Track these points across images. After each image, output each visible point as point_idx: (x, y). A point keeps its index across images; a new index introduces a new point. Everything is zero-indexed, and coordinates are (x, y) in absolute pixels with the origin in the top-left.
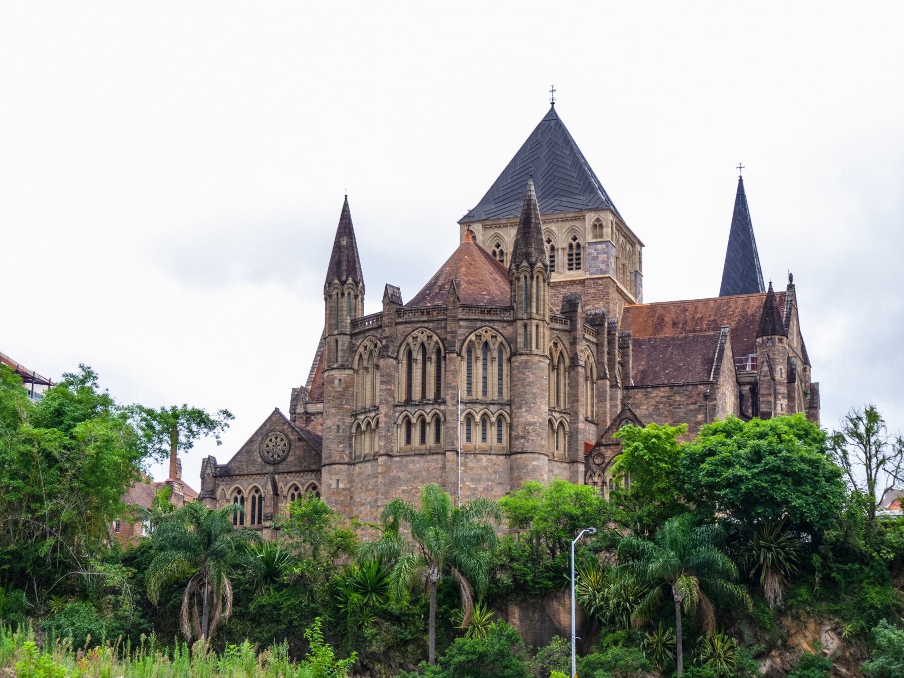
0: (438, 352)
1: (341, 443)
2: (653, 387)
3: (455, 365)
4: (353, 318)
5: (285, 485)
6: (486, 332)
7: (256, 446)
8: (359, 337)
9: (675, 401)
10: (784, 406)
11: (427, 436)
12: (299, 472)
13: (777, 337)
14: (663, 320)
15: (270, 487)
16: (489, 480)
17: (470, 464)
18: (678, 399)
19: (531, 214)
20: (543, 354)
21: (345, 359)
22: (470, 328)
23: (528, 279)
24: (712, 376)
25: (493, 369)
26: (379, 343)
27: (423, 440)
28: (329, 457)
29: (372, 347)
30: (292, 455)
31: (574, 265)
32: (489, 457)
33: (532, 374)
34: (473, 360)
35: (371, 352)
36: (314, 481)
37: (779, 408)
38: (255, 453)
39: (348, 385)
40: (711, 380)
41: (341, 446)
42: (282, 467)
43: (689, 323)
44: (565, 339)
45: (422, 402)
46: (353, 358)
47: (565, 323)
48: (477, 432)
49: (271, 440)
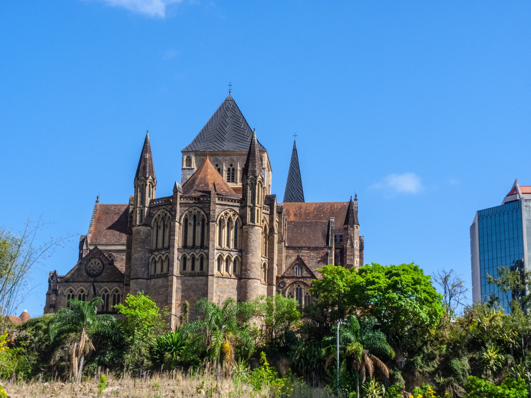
0: (203, 220)
1: (143, 267)
2: (309, 248)
3: (214, 229)
4: (151, 199)
5: (100, 289)
6: (230, 211)
7: (83, 267)
8: (155, 209)
9: (311, 256)
10: (358, 262)
11: (195, 267)
12: (109, 282)
13: (355, 225)
14: (288, 212)
15: (92, 290)
16: (229, 292)
17: (220, 283)
18: (312, 254)
19: (255, 149)
20: (260, 225)
21: (147, 221)
22: (221, 209)
23: (254, 184)
24: (330, 244)
25: (232, 232)
26: (169, 214)
27: (193, 268)
28: (136, 275)
29: (164, 215)
30: (105, 273)
31: (231, 179)
32: (230, 279)
33: (255, 236)
34: (222, 226)
35: (163, 218)
36: (118, 288)
37: (355, 263)
38: (82, 270)
39: (149, 235)
40: (330, 245)
41: (143, 269)
42: (98, 279)
43: (303, 215)
44: (267, 217)
45: (194, 247)
46: (151, 221)
47: (268, 210)
48: (223, 266)
49: (92, 263)
